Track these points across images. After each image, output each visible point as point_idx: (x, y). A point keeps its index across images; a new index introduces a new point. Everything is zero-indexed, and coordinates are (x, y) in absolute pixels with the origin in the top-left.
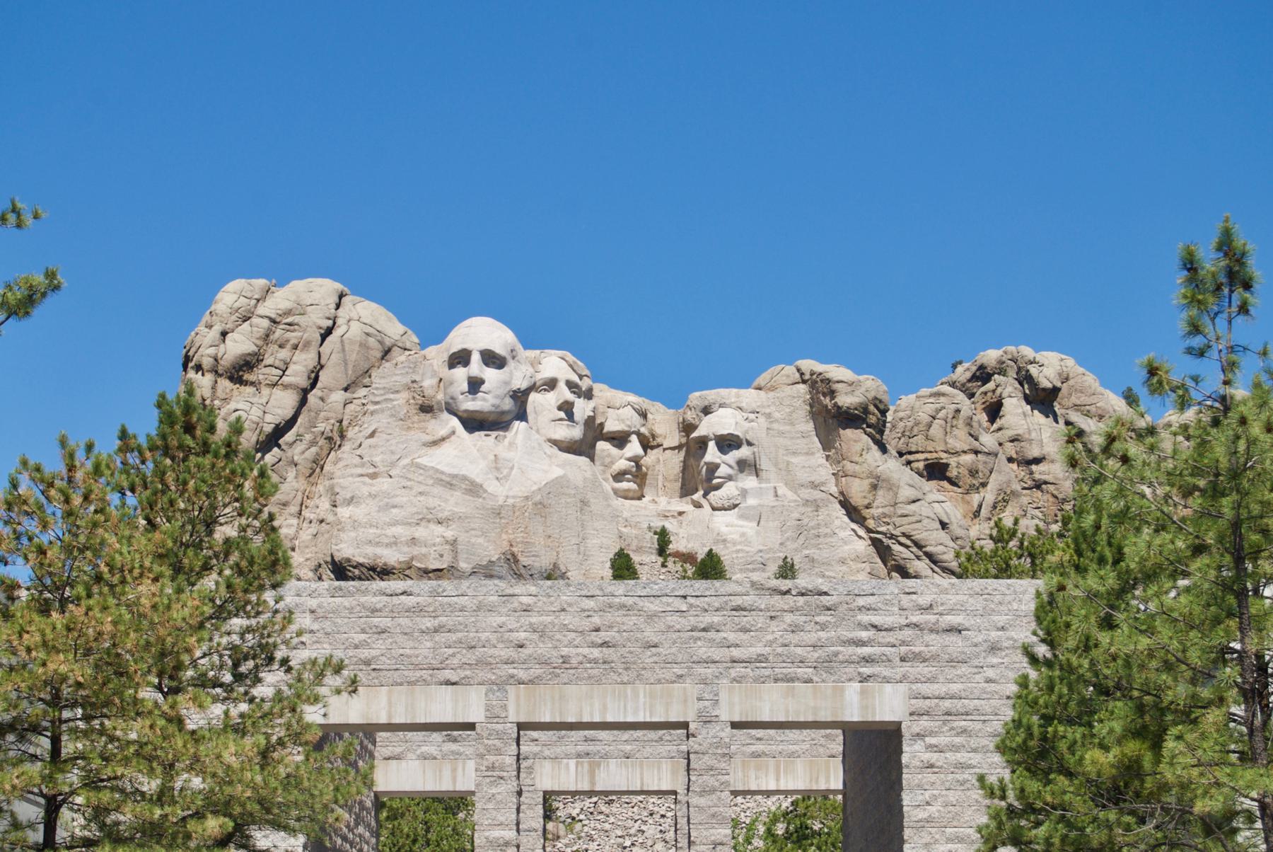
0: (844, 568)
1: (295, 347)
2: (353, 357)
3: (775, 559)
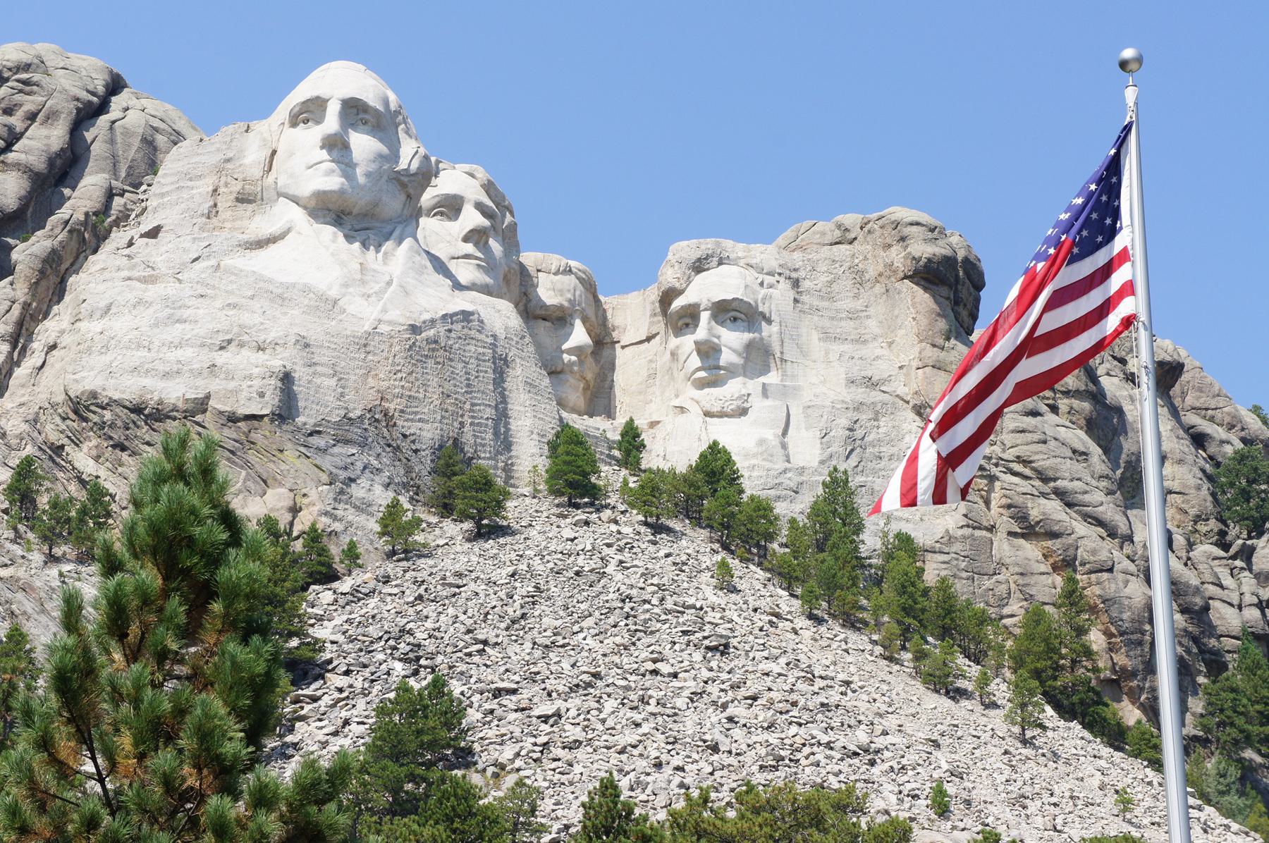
1: (32, 117)
2: (131, 152)
3: (812, 486)
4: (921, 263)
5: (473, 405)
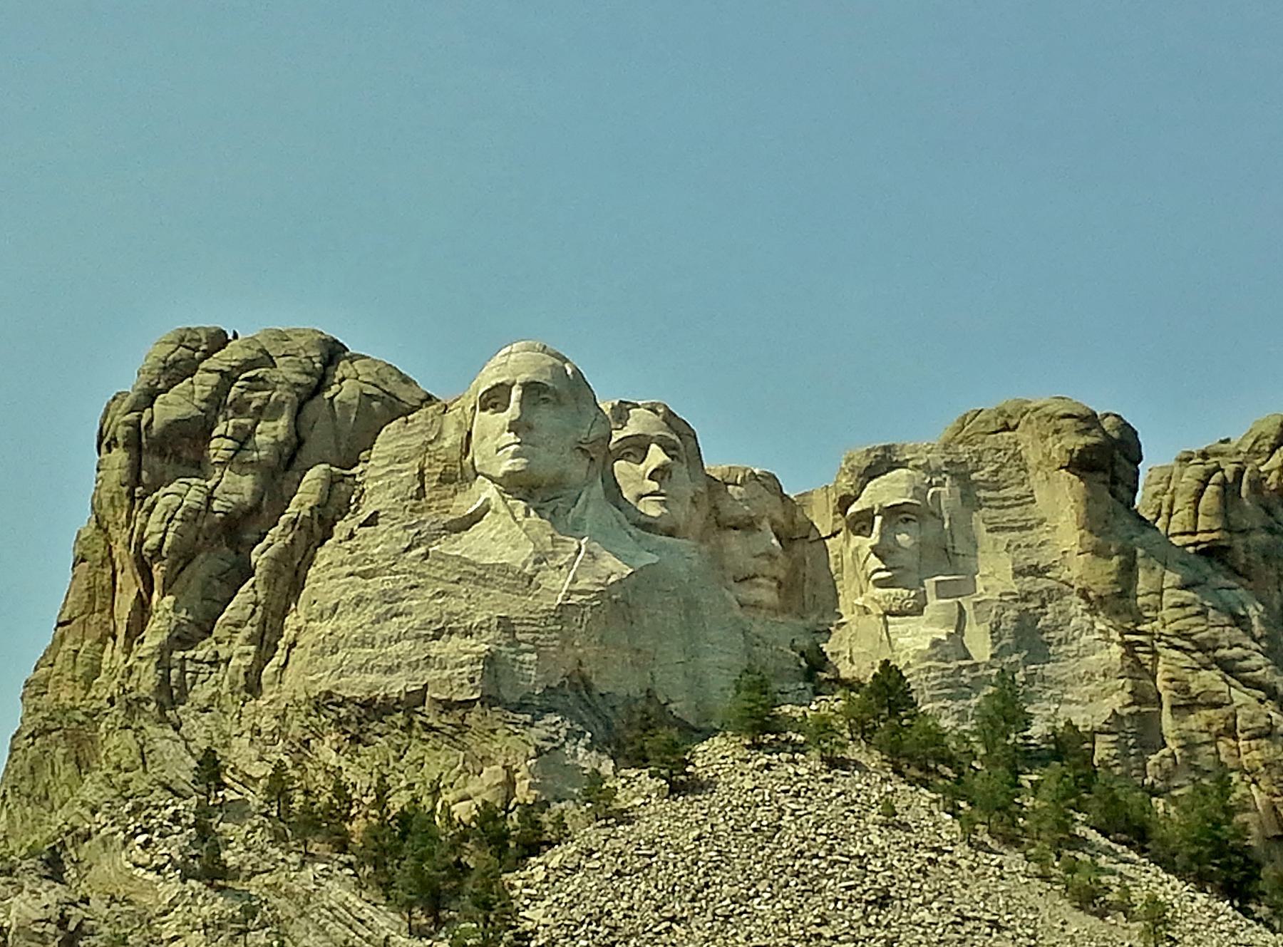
0: (1092, 687)
4: (1075, 455)
5: (663, 653)
